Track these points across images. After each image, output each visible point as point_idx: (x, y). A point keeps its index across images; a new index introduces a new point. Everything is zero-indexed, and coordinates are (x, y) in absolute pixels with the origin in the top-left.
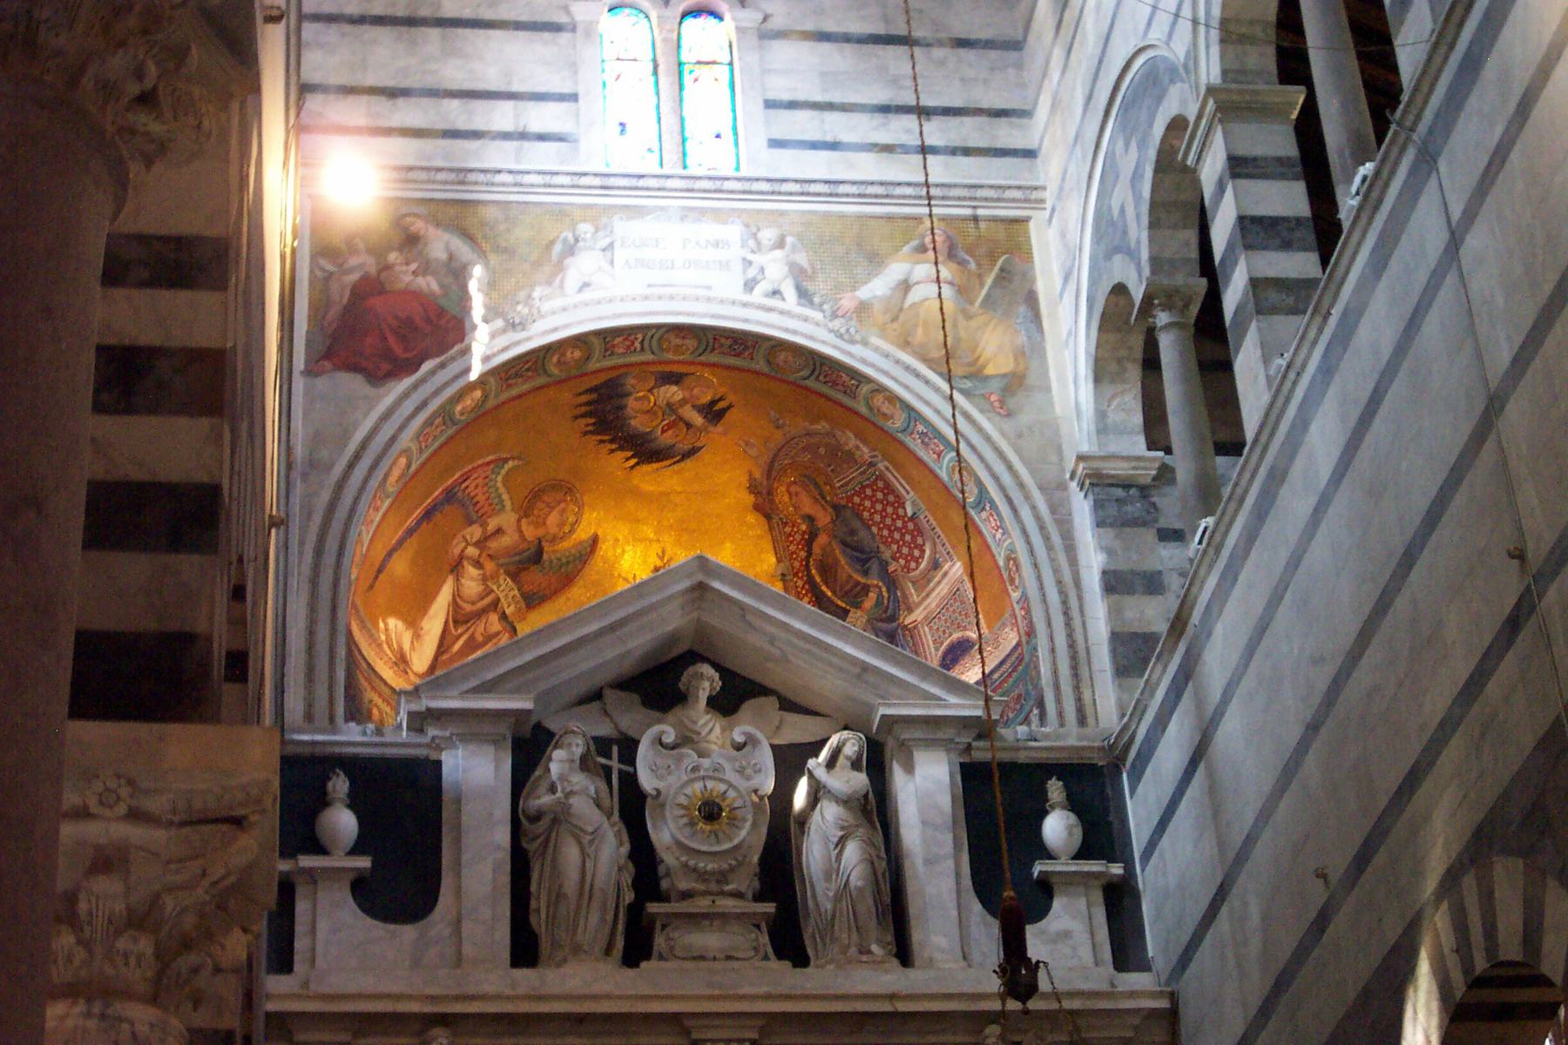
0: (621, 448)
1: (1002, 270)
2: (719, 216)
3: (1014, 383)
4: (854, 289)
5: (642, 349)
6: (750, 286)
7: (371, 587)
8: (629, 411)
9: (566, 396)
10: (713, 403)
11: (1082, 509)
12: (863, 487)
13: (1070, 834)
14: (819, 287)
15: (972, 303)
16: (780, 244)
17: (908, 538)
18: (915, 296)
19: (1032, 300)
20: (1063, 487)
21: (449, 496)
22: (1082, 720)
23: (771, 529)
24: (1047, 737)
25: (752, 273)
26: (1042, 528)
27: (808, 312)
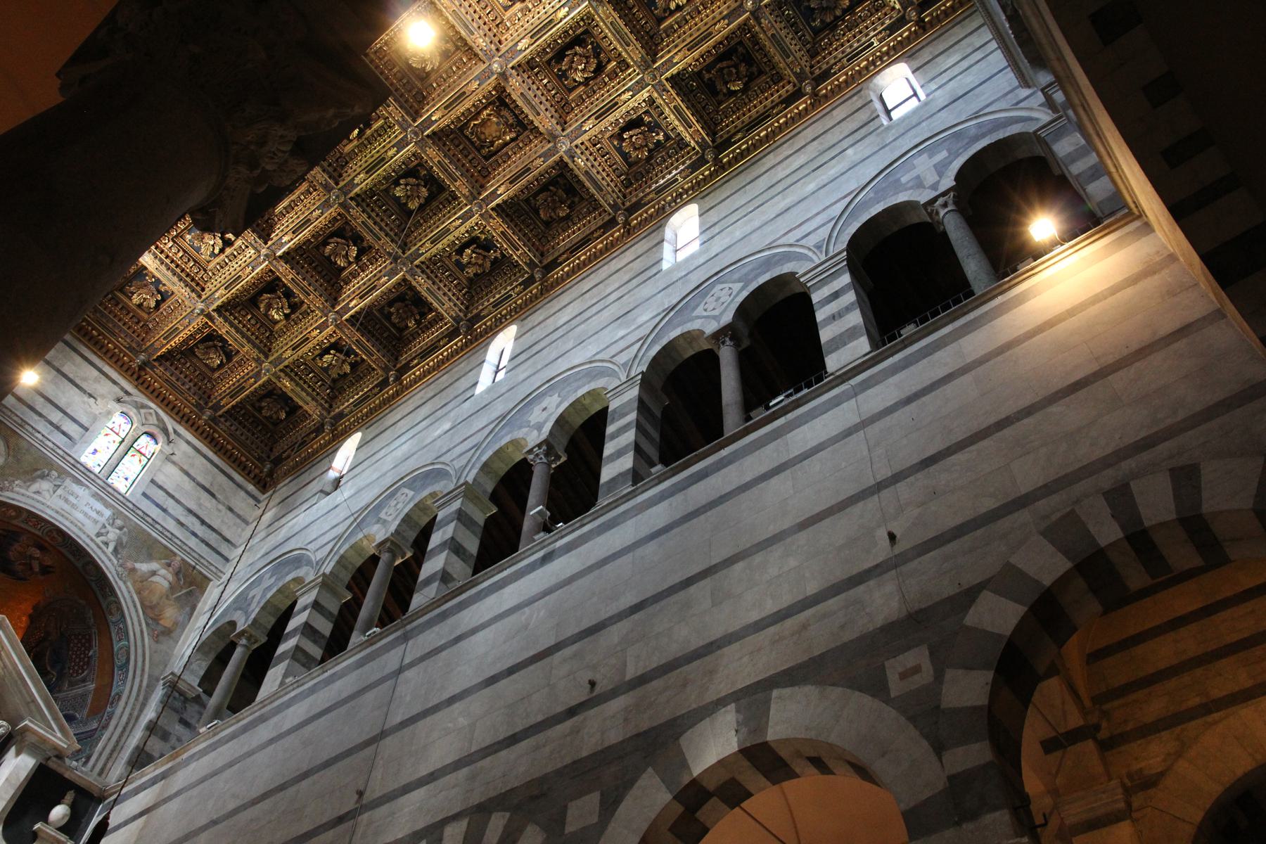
1: (191, 591)
2: (107, 505)
3: (167, 632)
4: (136, 561)
5: (40, 530)
6: (98, 535)
10: (48, 566)
11: (159, 693)
13: (63, 818)
15: (172, 595)
16: (121, 529)
18: (155, 579)
19: (193, 608)
20: (158, 680)
22: (100, 774)
24: (82, 772)
25: (103, 531)
26: (139, 690)
27: (113, 558)
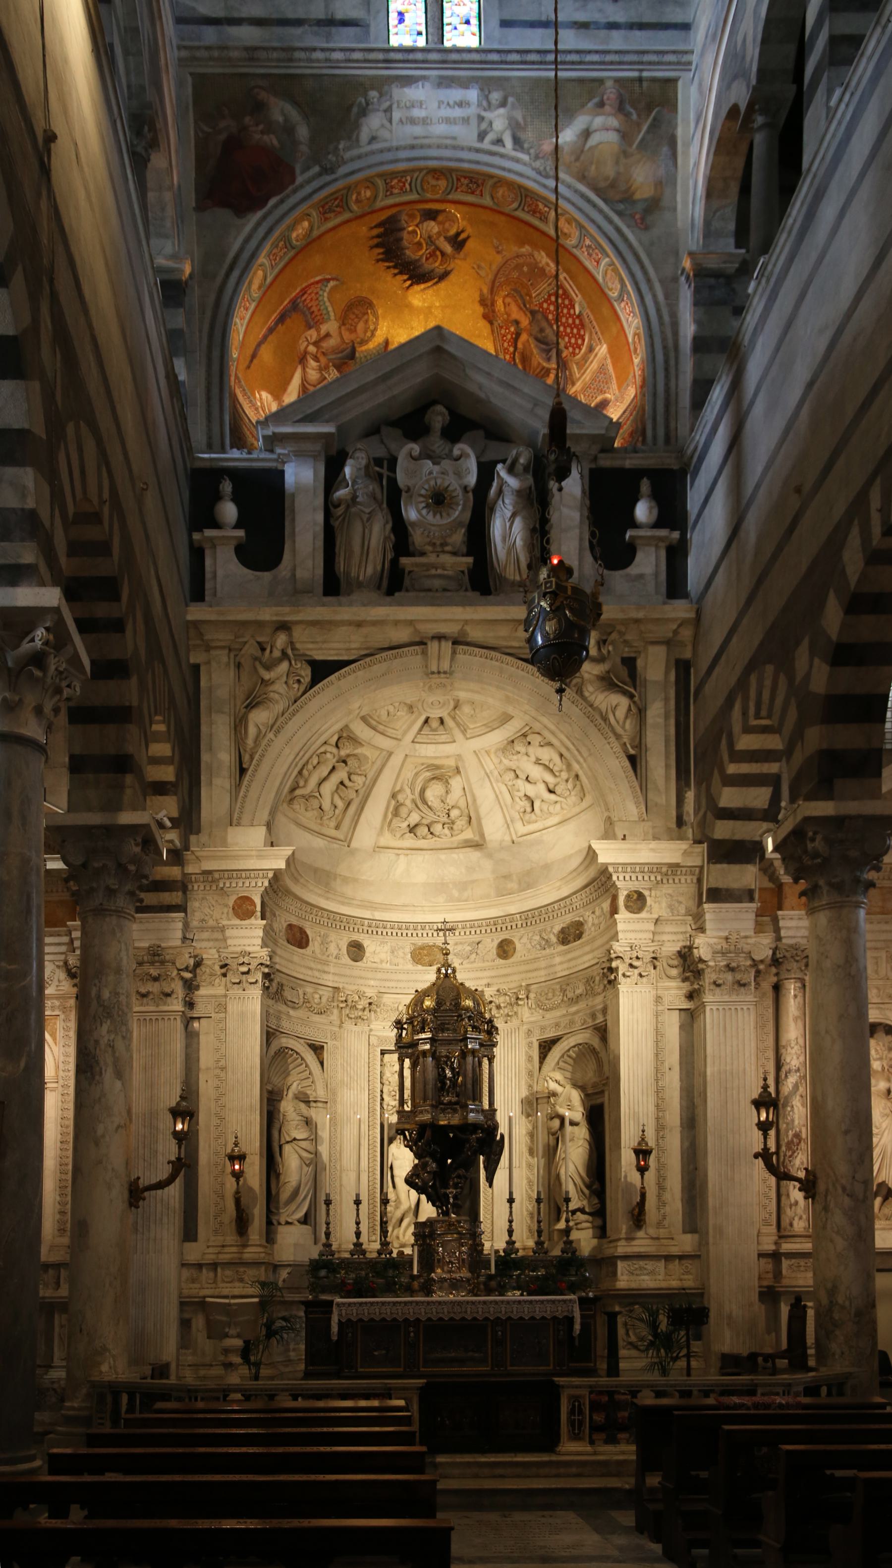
0: (401, 273)
1: (655, 119)
2: (465, 84)
3: (654, 205)
5: (411, 190)
6: (481, 136)
7: (248, 367)
8: (405, 243)
9: (363, 230)
10: (458, 234)
12: (550, 296)
14: (528, 136)
15: (630, 145)
16: (503, 104)
17: (575, 331)
18: (593, 140)
21: (294, 306)
23: (493, 331)
25: (484, 126)
27: (520, 155)
